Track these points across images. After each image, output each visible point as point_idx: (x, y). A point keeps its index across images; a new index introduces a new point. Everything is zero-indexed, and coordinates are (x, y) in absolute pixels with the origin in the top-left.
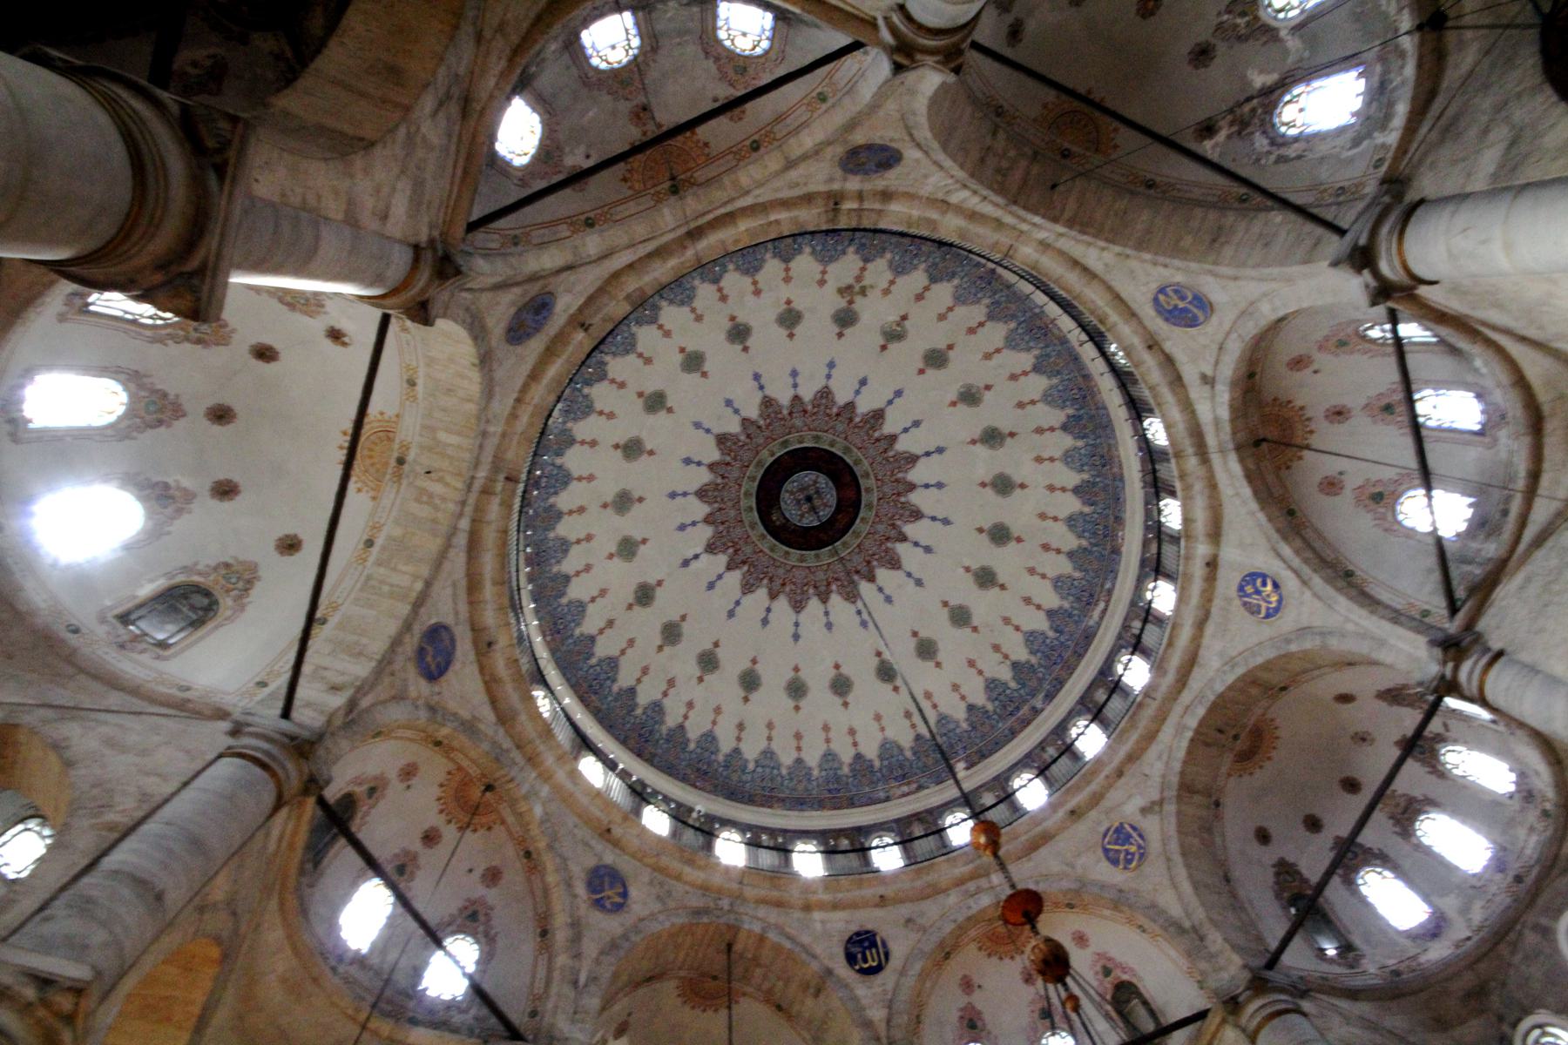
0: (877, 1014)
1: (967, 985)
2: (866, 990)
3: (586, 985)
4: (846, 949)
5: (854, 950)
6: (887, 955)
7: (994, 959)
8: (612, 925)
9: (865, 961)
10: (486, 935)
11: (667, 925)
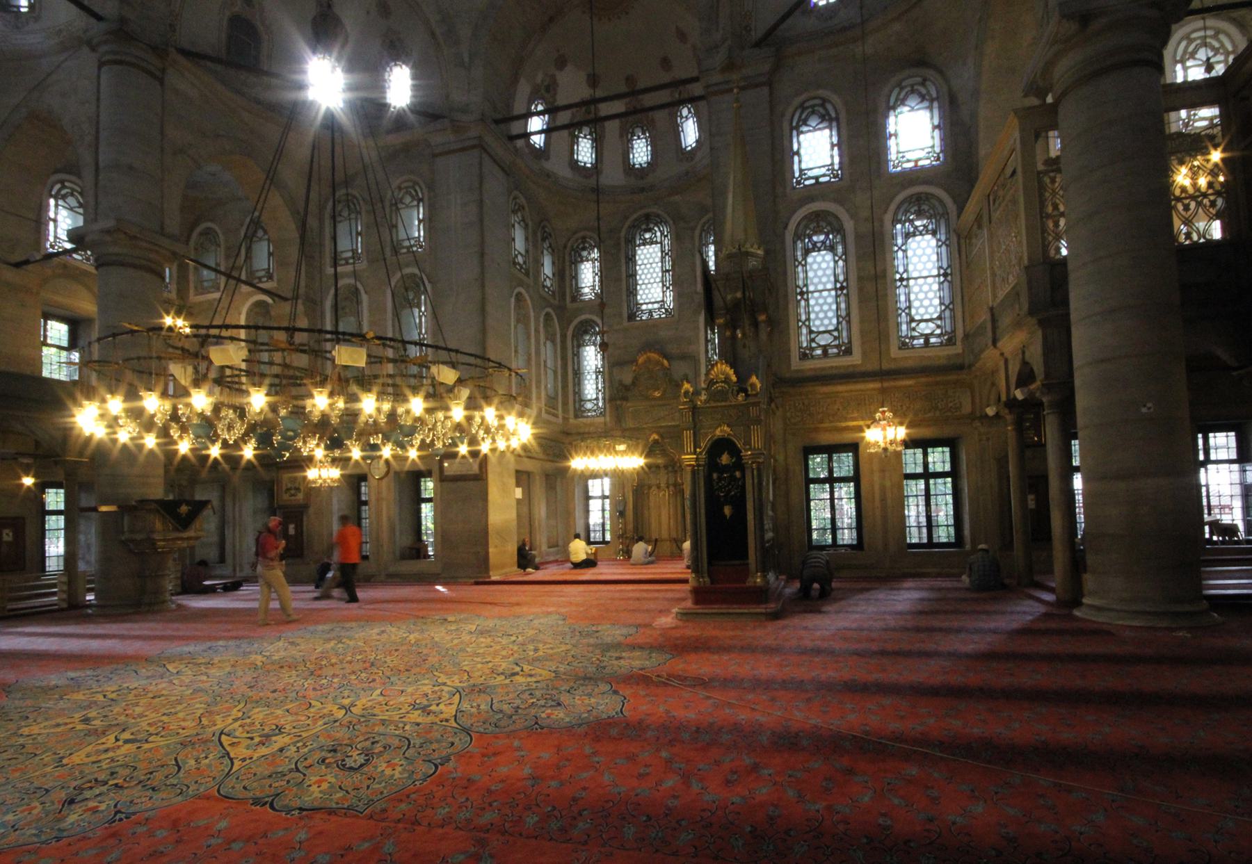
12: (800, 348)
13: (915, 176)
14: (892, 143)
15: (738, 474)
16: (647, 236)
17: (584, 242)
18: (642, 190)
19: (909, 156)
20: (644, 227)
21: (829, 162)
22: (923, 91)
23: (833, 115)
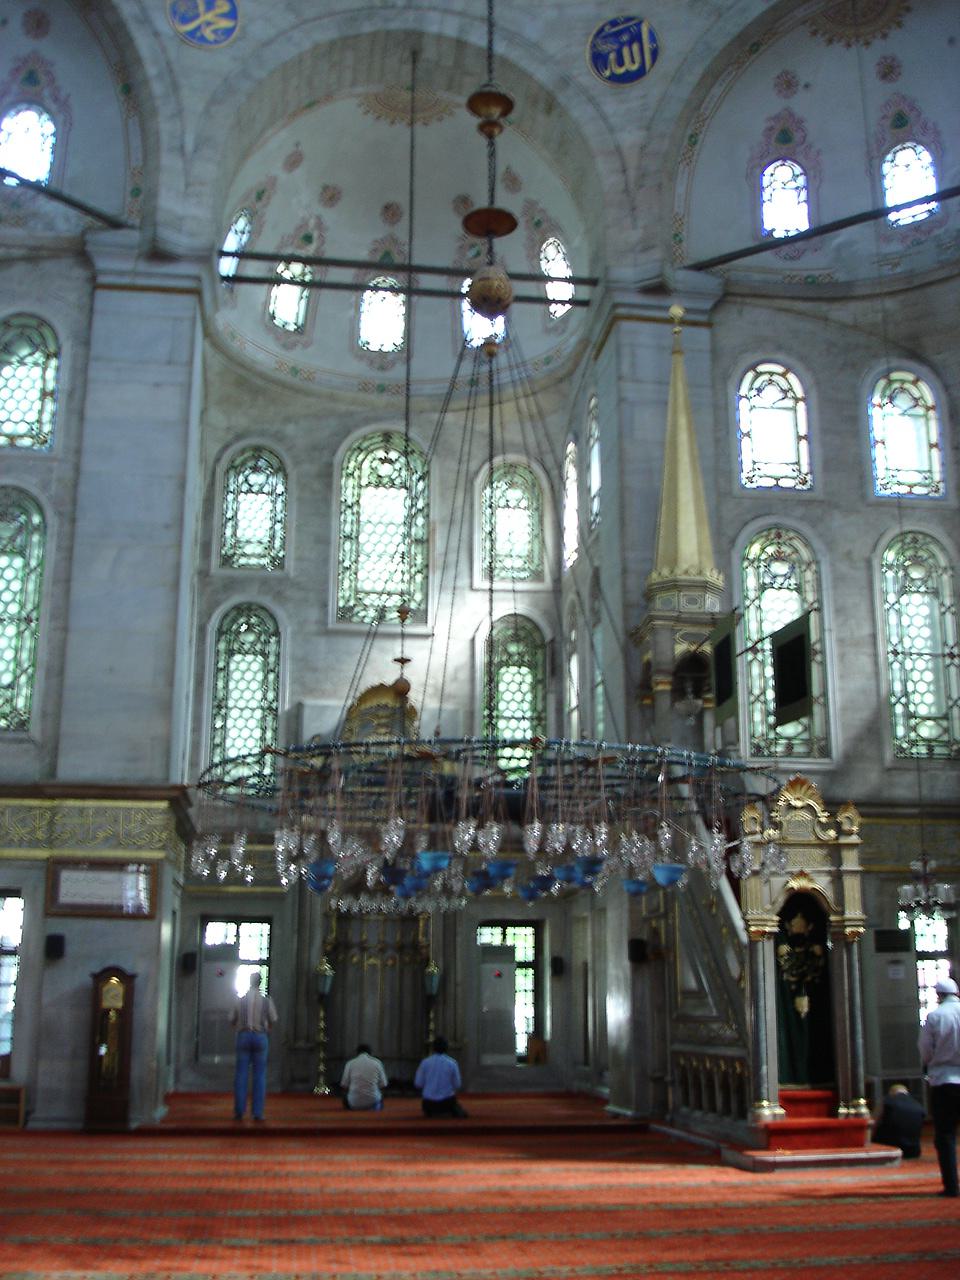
0: (630, 138)
1: (787, 84)
2: (620, 105)
3: (196, 150)
4: (594, 46)
5: (604, 48)
6: (655, 54)
7: (838, 47)
8: (221, 60)
9: (621, 63)
10: (56, 100)
11: (307, 45)
12: (753, 736)
13: (900, 505)
14: (878, 452)
15: (817, 949)
16: (385, 470)
17: (258, 458)
18: (382, 389)
19: (901, 477)
20: (381, 454)
21: (795, 460)
22: (896, 385)
23: (800, 393)
